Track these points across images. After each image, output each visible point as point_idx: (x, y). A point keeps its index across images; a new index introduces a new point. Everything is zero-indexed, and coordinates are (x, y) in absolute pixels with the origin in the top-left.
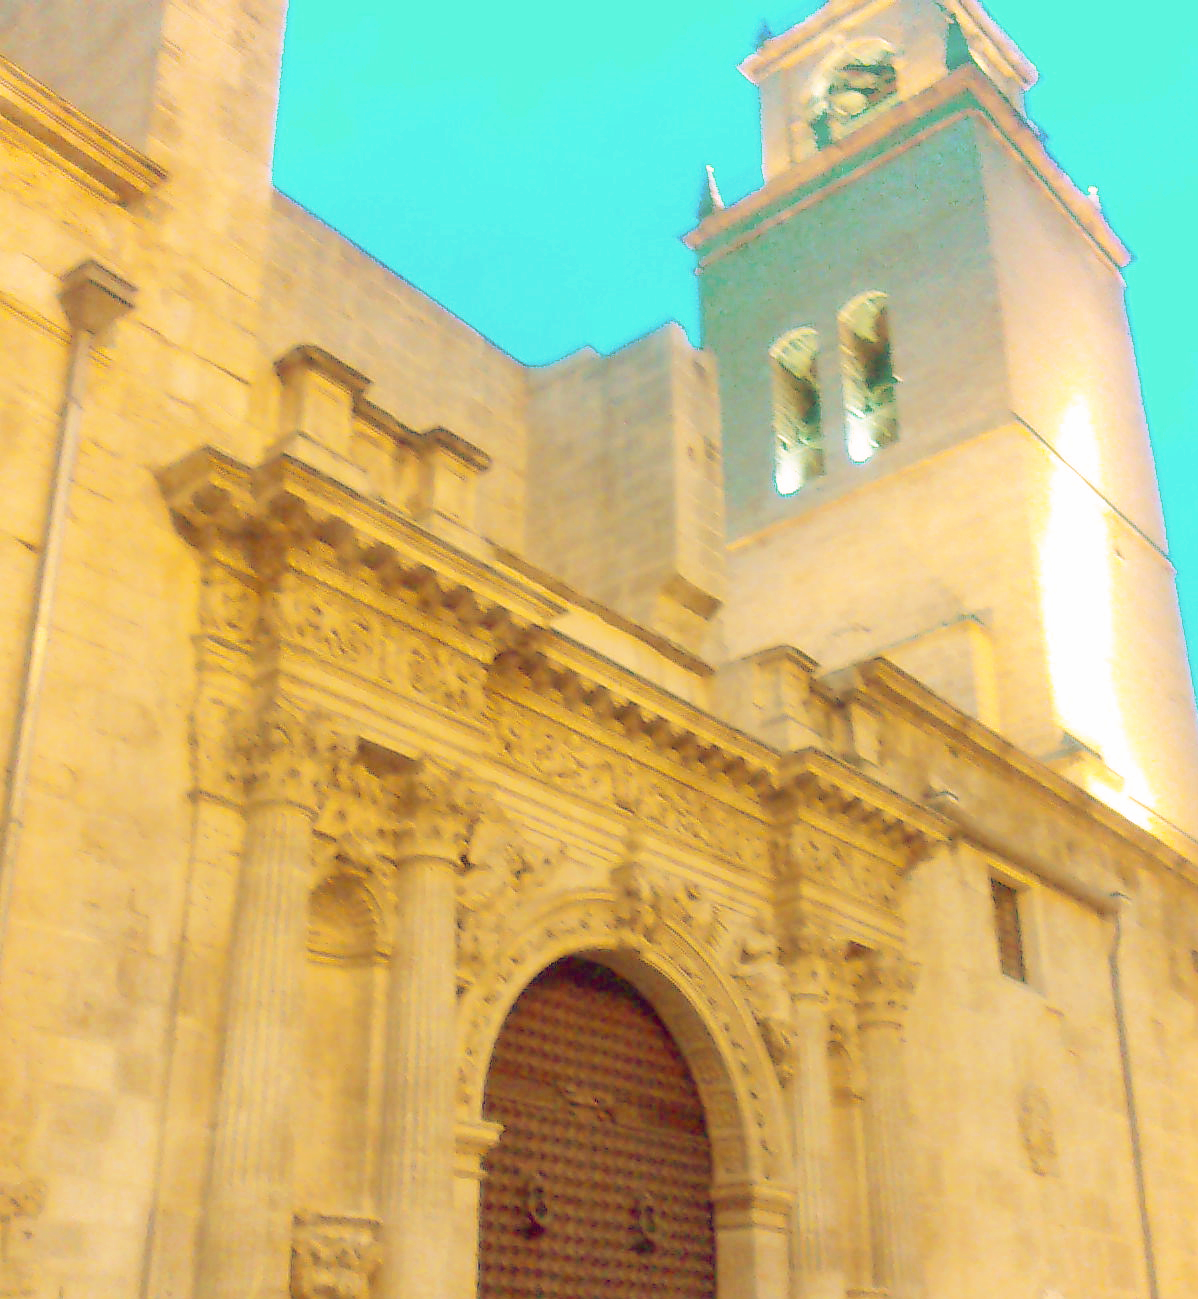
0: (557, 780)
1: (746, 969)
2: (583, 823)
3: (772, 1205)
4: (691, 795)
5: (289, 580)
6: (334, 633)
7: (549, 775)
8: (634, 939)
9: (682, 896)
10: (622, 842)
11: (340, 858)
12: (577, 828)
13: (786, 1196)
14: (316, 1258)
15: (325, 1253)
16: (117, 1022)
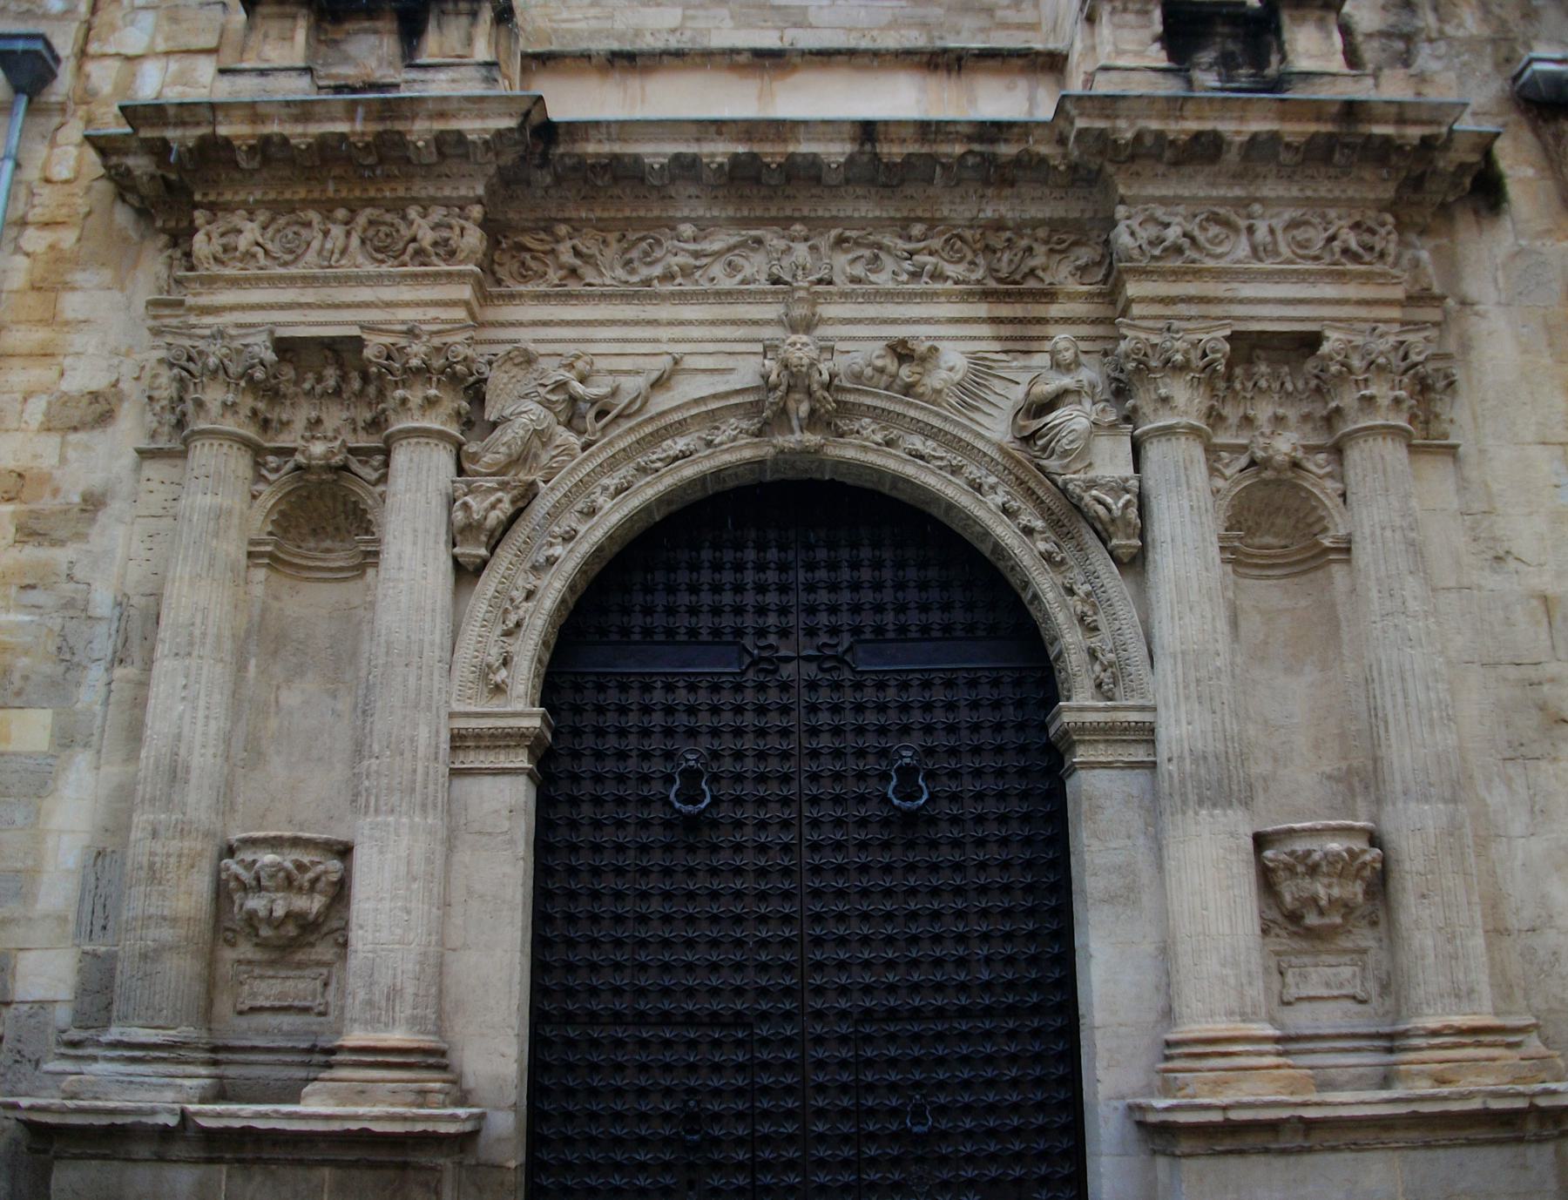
0: (669, 288)
1: (1035, 424)
2: (702, 323)
3: (1110, 733)
4: (917, 229)
5: (200, 216)
6: (258, 244)
7: (647, 282)
8: (795, 439)
9: (891, 364)
10: (780, 322)
11: (298, 467)
12: (696, 332)
13: (1134, 717)
14: (244, 888)
15: (246, 876)
16: (58, 689)
